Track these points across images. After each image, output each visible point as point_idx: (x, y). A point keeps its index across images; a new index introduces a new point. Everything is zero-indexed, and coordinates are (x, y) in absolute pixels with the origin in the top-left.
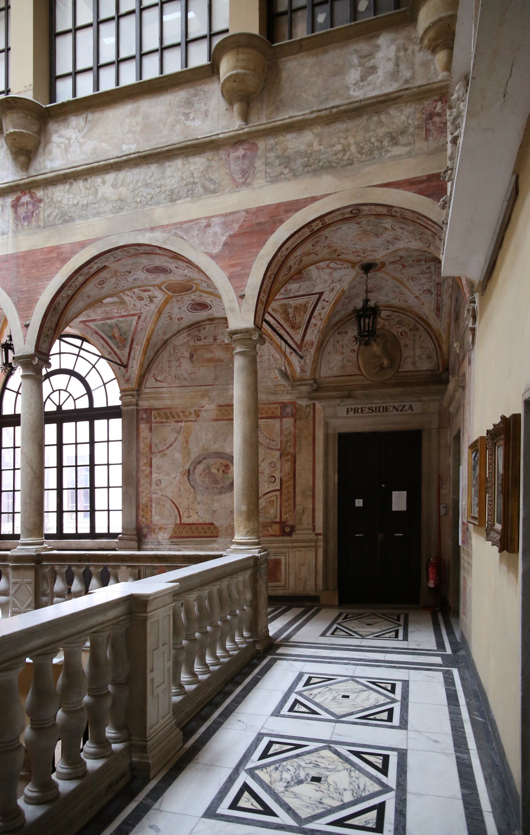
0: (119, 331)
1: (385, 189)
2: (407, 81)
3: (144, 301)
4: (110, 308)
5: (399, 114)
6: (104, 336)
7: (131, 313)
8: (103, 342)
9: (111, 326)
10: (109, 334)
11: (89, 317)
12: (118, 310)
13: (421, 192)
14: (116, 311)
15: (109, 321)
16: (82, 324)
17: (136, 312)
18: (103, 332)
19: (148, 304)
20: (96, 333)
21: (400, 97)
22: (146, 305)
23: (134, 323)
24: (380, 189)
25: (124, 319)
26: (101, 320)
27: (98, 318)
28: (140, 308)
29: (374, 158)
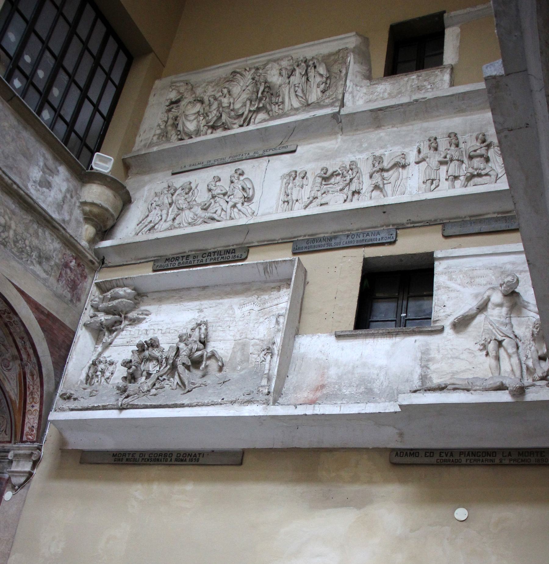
1: (19, 294)
2: (64, 221)
5: (50, 241)
13: (40, 322)
21: (58, 229)
24: (15, 291)
29: (22, 259)
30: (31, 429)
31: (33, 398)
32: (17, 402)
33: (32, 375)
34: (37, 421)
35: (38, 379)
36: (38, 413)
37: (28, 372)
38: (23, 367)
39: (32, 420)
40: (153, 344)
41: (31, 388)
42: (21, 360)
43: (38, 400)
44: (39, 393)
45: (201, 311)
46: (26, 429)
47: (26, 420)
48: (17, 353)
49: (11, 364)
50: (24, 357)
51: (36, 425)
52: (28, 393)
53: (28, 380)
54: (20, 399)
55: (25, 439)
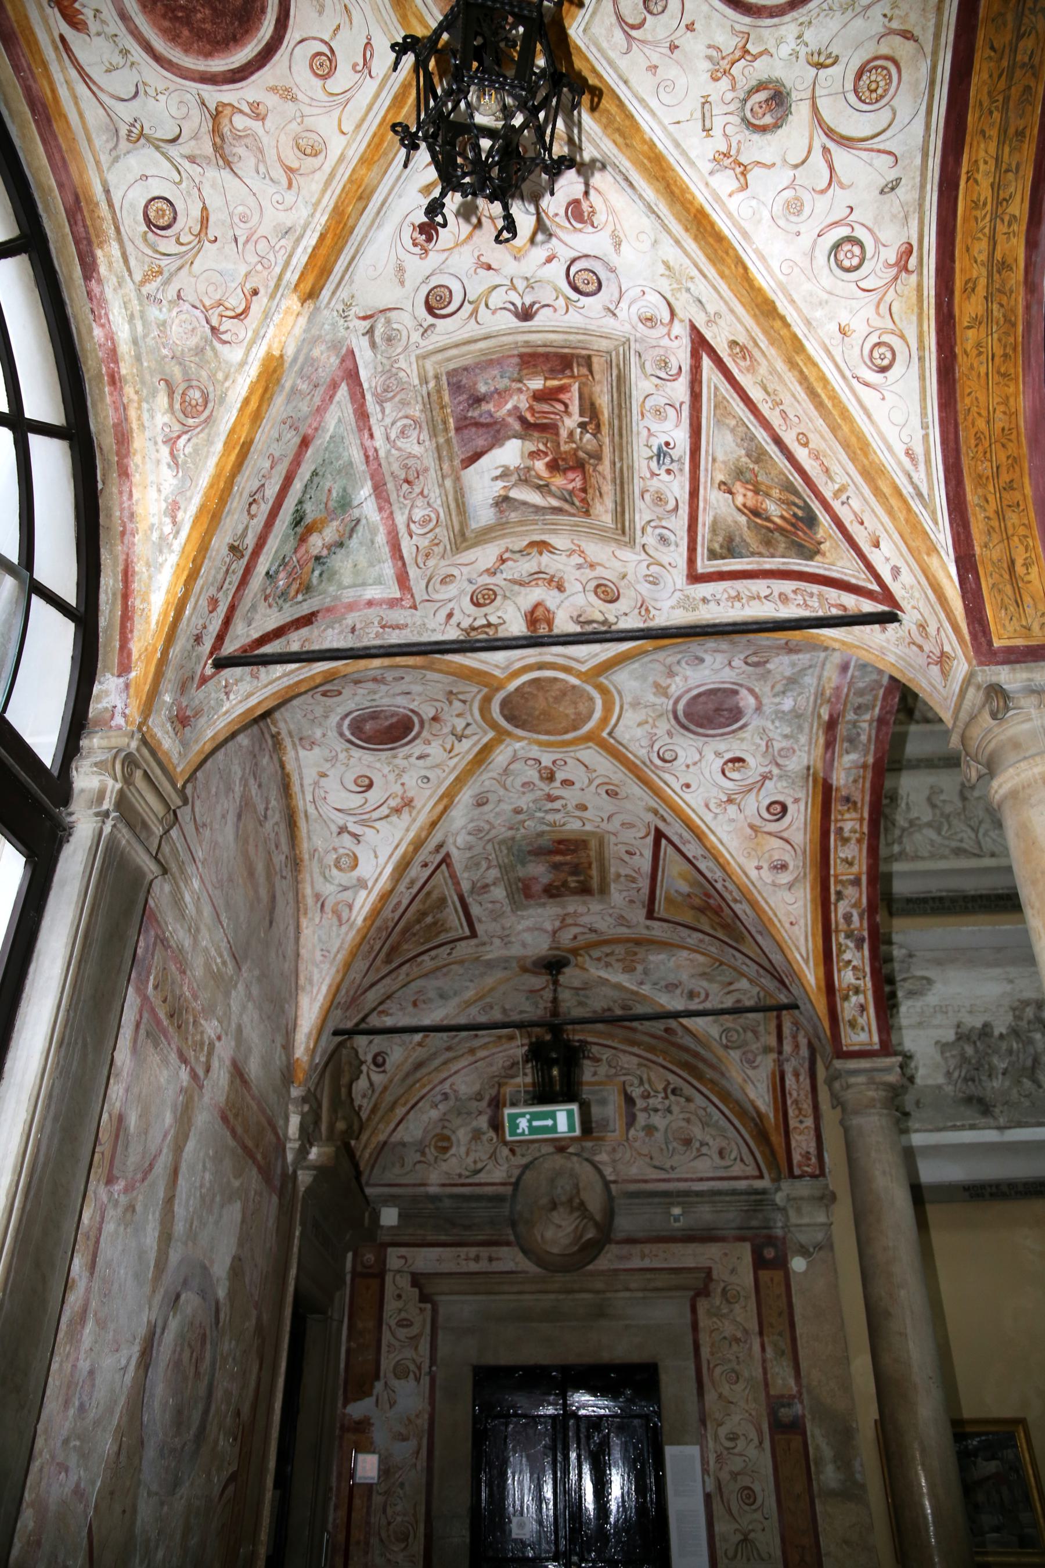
0: (329, 548)
3: (471, 609)
4: (435, 494)
6: (297, 486)
7: (413, 572)
8: (272, 491)
9: (345, 503)
10: (312, 512)
11: (381, 402)
12: (425, 521)
14: (418, 514)
15: (364, 492)
16: (334, 361)
17: (418, 585)
18: (315, 474)
19: (453, 621)
20: (305, 443)
22: (450, 616)
23: (372, 593)
25: (386, 550)
26: (370, 458)
27: (379, 442)
28: (436, 597)
30: (807, 1156)
31: (800, 1110)
32: (772, 1116)
33: (797, 1075)
34: (813, 1144)
35: (808, 1081)
36: (812, 1133)
37: (788, 1069)
38: (780, 1063)
39: (802, 1142)
40: (986, 1031)
41: (795, 1094)
42: (780, 1052)
43: (810, 1111)
44: (810, 1101)
45: (1011, 981)
46: (796, 1158)
47: (793, 1144)
48: (773, 1041)
49: (759, 1059)
50: (787, 1048)
51: (813, 1150)
52: (789, 1102)
53: (787, 1082)
54: (776, 1110)
55: (797, 1171)
